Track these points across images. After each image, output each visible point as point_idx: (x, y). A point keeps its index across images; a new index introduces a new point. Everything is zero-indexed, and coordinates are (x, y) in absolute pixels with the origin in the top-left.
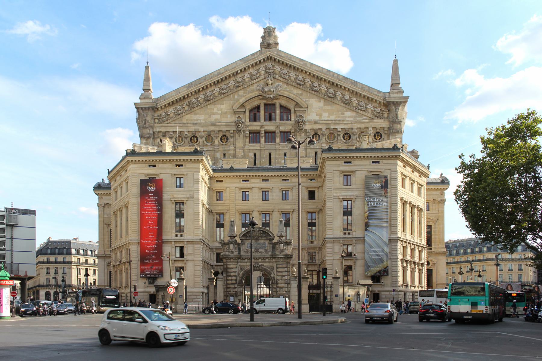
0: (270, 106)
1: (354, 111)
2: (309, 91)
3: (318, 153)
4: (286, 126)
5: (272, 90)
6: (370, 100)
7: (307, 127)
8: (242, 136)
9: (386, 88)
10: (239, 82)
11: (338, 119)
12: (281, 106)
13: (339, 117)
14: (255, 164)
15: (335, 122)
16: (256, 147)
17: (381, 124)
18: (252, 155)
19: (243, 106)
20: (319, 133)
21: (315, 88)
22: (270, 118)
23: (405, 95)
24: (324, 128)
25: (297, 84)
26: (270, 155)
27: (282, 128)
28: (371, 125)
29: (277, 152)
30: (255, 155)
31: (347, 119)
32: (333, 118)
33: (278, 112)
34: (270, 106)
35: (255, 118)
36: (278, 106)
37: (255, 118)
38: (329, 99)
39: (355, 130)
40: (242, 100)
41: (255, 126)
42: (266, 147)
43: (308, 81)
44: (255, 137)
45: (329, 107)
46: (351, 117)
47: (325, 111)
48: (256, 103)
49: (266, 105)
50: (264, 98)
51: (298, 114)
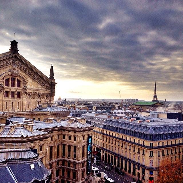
0: (13, 79)
1: (41, 85)
2: (28, 74)
3: (30, 103)
4: (20, 90)
5: (17, 73)
6: (46, 82)
7: (27, 91)
8: (2, 93)
9: (49, 77)
10: (2, 66)
11: (36, 88)
12: (17, 80)
13: (37, 87)
14: (6, 108)
15: (36, 90)
16: (7, 99)
17: (49, 92)
18: (5, 103)
19: (3, 78)
20: (31, 94)
21: (30, 74)
22: (13, 85)
23: (56, 82)
24: (32, 92)
25: (24, 71)
26: (12, 103)
27: (18, 91)
28: (46, 92)
29: (16, 102)
30: (6, 103)
31: (39, 89)
32: (35, 87)
33: (16, 83)
34: (13, 79)
35: (7, 85)
36: (17, 80)
37: (7, 85)
38: (34, 79)
39: (42, 94)
40: (3, 75)
41: (7, 89)
42: (12, 100)
43: (28, 70)
44: (7, 94)
45: (34, 83)
46: (40, 88)
47: (33, 84)
48: (8, 77)
49: (12, 78)
50: (12, 76)
51: (24, 85)
